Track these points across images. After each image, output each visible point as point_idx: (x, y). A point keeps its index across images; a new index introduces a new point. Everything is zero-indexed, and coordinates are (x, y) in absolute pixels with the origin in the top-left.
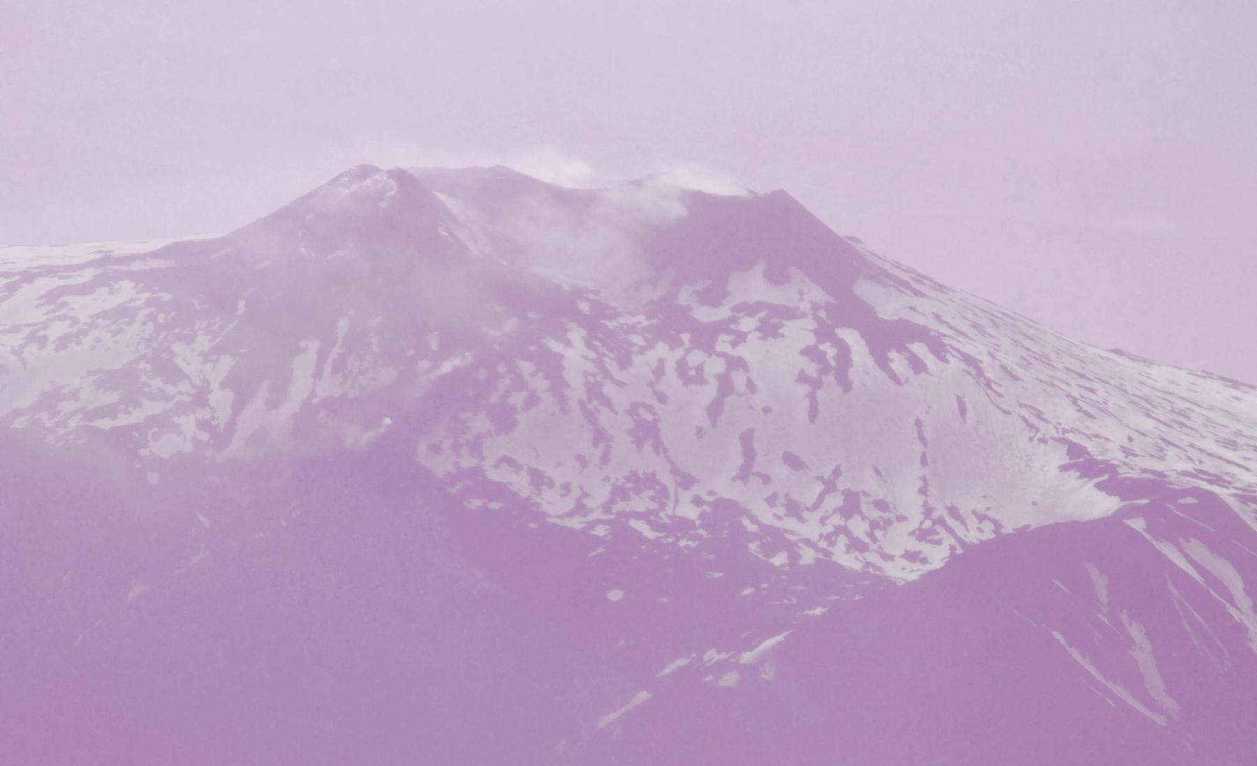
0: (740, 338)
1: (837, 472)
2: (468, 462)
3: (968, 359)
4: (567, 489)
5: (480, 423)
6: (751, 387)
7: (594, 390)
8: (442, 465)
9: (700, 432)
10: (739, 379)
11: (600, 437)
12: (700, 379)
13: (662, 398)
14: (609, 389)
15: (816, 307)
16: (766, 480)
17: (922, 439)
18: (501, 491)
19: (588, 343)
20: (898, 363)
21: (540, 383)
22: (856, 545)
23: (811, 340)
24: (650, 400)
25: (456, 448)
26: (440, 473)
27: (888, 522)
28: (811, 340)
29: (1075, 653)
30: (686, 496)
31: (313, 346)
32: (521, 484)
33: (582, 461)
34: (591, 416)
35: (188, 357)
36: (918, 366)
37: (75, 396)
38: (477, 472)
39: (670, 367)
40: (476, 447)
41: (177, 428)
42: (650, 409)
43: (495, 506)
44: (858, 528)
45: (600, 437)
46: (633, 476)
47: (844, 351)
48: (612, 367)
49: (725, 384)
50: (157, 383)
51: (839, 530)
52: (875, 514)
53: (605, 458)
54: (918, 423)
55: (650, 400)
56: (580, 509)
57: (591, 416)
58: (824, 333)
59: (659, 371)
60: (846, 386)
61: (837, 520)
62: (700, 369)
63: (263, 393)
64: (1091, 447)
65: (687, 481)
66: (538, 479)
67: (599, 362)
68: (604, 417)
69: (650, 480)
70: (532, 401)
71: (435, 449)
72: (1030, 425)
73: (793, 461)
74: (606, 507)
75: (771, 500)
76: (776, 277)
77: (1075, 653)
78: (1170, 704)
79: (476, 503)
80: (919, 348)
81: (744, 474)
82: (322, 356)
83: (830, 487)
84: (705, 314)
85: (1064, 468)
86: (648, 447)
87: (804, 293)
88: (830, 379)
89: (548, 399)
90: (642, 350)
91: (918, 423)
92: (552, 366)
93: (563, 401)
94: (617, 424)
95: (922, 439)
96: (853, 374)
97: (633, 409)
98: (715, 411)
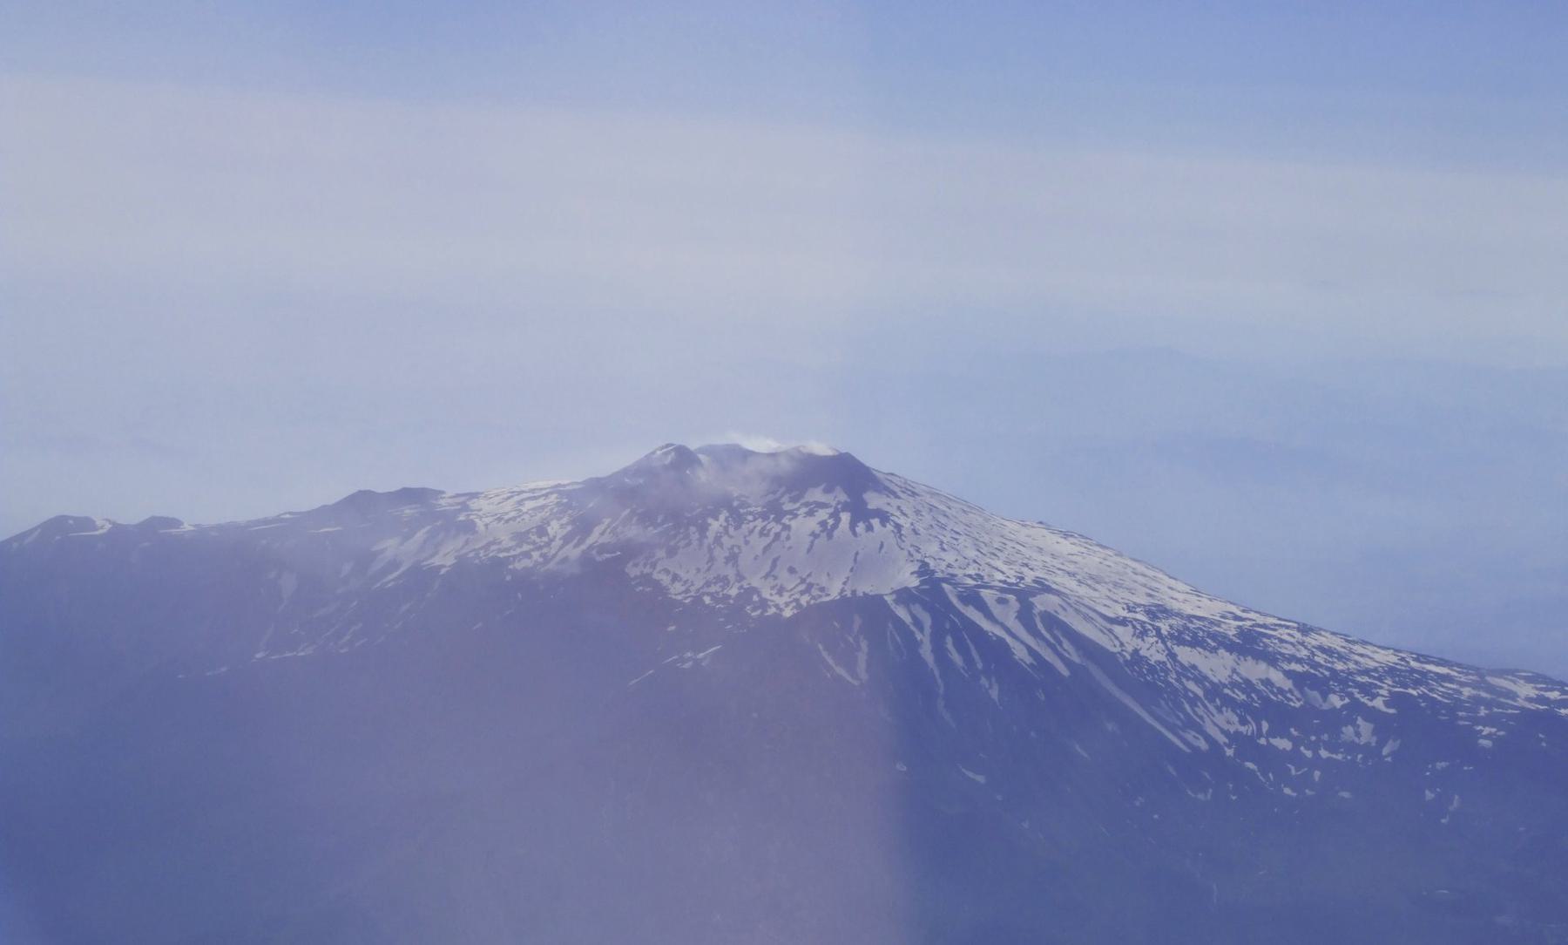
0: (796, 516)
2: (647, 570)
3: (898, 527)
6: (788, 538)
7: (718, 540)
10: (784, 534)
12: (767, 535)
13: (747, 543)
14: (725, 539)
16: (775, 578)
20: (861, 527)
29: (825, 654)
32: (665, 580)
33: (698, 570)
34: (710, 550)
35: (554, 528)
36: (870, 528)
38: (650, 575)
40: (654, 566)
45: (712, 559)
47: (838, 521)
49: (777, 535)
50: (534, 538)
56: (687, 591)
57: (710, 550)
60: (830, 536)
65: (740, 577)
66: (675, 578)
67: (726, 529)
68: (718, 552)
71: (636, 565)
72: (910, 554)
73: (792, 570)
77: (825, 654)
78: (864, 676)
80: (875, 522)
81: (766, 577)
83: (803, 581)
84: (788, 506)
89: (695, 543)
92: (703, 529)
94: (721, 554)
96: (836, 533)
98: (766, 549)
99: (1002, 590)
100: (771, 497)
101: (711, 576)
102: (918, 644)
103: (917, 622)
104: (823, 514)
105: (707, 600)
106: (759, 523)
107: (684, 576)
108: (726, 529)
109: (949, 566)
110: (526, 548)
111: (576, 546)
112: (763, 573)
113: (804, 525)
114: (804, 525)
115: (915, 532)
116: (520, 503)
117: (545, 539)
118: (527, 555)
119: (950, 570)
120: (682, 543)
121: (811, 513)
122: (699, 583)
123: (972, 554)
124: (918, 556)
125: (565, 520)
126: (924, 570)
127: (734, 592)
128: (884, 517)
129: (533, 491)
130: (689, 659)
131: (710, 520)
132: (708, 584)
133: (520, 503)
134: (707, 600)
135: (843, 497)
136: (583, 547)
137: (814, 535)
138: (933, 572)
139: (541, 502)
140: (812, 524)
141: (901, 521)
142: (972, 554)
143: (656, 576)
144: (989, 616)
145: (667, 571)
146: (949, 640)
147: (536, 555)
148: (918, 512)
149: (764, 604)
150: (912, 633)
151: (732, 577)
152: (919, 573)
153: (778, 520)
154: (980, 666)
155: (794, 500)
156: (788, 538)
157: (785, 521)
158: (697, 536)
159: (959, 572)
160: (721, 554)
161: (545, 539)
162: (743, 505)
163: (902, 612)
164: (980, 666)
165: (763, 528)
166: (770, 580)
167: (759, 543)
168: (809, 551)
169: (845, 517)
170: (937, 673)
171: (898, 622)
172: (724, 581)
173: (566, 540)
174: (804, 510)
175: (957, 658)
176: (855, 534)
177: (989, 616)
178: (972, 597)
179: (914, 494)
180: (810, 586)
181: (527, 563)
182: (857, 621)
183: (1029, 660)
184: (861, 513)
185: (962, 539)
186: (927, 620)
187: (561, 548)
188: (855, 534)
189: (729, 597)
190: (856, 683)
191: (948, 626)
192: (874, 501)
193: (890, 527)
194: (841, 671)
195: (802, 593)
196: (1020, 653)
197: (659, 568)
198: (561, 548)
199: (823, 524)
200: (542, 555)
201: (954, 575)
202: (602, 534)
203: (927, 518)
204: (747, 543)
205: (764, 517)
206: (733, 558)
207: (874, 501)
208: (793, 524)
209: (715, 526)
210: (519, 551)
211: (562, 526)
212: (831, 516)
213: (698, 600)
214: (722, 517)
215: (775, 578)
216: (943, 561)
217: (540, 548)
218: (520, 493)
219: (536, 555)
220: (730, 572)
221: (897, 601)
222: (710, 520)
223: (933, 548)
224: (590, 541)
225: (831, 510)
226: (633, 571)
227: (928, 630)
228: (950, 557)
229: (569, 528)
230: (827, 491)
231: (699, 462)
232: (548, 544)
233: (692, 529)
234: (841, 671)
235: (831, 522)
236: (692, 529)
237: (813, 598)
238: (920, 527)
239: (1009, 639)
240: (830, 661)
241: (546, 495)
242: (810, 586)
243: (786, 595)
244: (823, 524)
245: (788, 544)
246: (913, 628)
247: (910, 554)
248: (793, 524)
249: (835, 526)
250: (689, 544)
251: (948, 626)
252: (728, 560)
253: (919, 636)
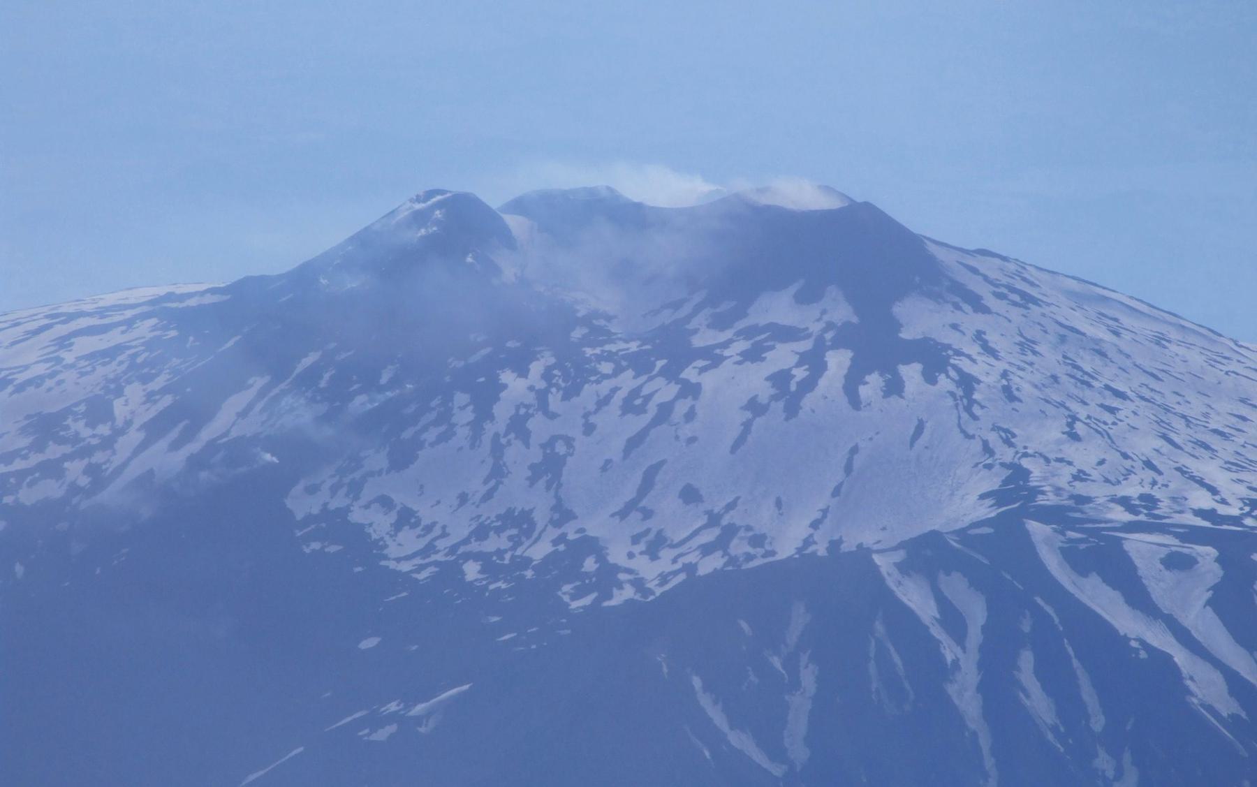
1: (731, 506)
2: (335, 504)
3: (967, 383)
4: (429, 529)
6: (690, 416)
7: (518, 426)
10: (682, 408)
12: (641, 410)
13: (589, 429)
17: (848, 469)
19: (547, 375)
20: (872, 386)
21: (464, 417)
29: (705, 701)
30: (553, 533)
31: (258, 382)
32: (380, 523)
33: (463, 499)
36: (894, 387)
40: (355, 489)
42: (569, 441)
45: (498, 472)
53: (488, 496)
54: (855, 450)
56: (429, 549)
57: (498, 449)
60: (792, 410)
63: (174, 434)
65: (562, 514)
66: (406, 518)
67: (542, 396)
71: (312, 490)
72: (987, 449)
73: (690, 495)
77: (705, 701)
78: (799, 753)
79: (316, 546)
80: (911, 373)
82: (262, 394)
83: (713, 519)
86: (541, 484)
89: (463, 433)
91: (855, 450)
94: (520, 458)
96: (808, 401)
97: (553, 439)
98: (635, 442)
99: (1192, 535)
100: (666, 317)
101: (491, 512)
102: (946, 672)
103: (953, 620)
104: (783, 356)
105: (472, 571)
106: (627, 381)
107: (426, 514)
108: (542, 396)
109: (1080, 476)
111: (176, 446)
112: (617, 505)
113: (731, 385)
114: (731, 385)
115: (1009, 394)
116: (63, 342)
117: (104, 430)
118: (52, 469)
119: (1081, 488)
120: (430, 435)
121: (754, 355)
122: (461, 529)
123: (1146, 444)
124: (1007, 455)
126: (1015, 490)
127: (539, 551)
128: (934, 358)
129: (102, 312)
130: (393, 718)
131: (507, 377)
132: (481, 533)
133: (63, 342)
134: (472, 571)
135: (842, 312)
136: (193, 447)
137: (755, 407)
138: (1037, 491)
139: (115, 338)
140: (755, 380)
141: (983, 370)
142: (1146, 444)
143: (357, 516)
144: (1139, 599)
145: (386, 503)
146: (1027, 660)
148: (1027, 345)
149: (608, 577)
150: (938, 643)
151: (541, 517)
152: (998, 497)
153: (671, 374)
154: (1098, 723)
155: (719, 323)
156: (690, 416)
157: (690, 374)
158: (468, 415)
159: (1099, 492)
160: (520, 458)
161: (104, 430)
162: (599, 335)
163: (916, 597)
164: (1098, 723)
165: (635, 393)
166: (635, 524)
167: (616, 428)
168: (735, 448)
169: (838, 362)
170: (985, 742)
171: (902, 617)
172: (521, 523)
173: (155, 429)
174: (742, 345)
175: (1039, 703)
176: (855, 402)
177: (1139, 599)
178: (1103, 556)
179: (1028, 299)
180: (730, 532)
181: (51, 489)
182: (800, 618)
183: (1227, 706)
184: (879, 349)
185: (1125, 409)
186: (976, 612)
187: (143, 446)
188: (855, 402)
189: (526, 562)
190: (778, 770)
192: (919, 319)
193: (945, 383)
194: (741, 741)
195: (706, 550)
196: (1205, 687)
197: (368, 493)
198: (143, 446)
199: (780, 379)
200: (92, 470)
201: (1083, 500)
202: (243, 414)
203: (1050, 357)
204: (589, 429)
205: (640, 364)
206: (550, 468)
207: (919, 319)
208: (709, 381)
209: (515, 387)
210: (35, 459)
211: (150, 398)
212: (803, 359)
213: (450, 572)
214: (536, 368)
215: (648, 514)
216: (1066, 462)
217: (87, 451)
218: (71, 317)
220: (540, 504)
221: (904, 568)
222: (507, 377)
223: (1050, 434)
224: (206, 435)
225: (805, 346)
226: (301, 504)
227: (975, 636)
228: (1085, 455)
229: (168, 400)
230: (803, 298)
231: (508, 240)
232: (108, 443)
233: (461, 398)
234: (741, 741)
235: (800, 374)
236: (461, 398)
237: (733, 560)
238: (1024, 384)
239: (1180, 656)
240: (718, 718)
241: (129, 323)
242: (730, 532)
243: (666, 554)
244: (780, 379)
245: (687, 431)
246: (937, 632)
247: (987, 449)
248: (709, 381)
249: (809, 385)
250: (444, 438)
251: (1026, 627)
252: (536, 473)
253: (950, 652)
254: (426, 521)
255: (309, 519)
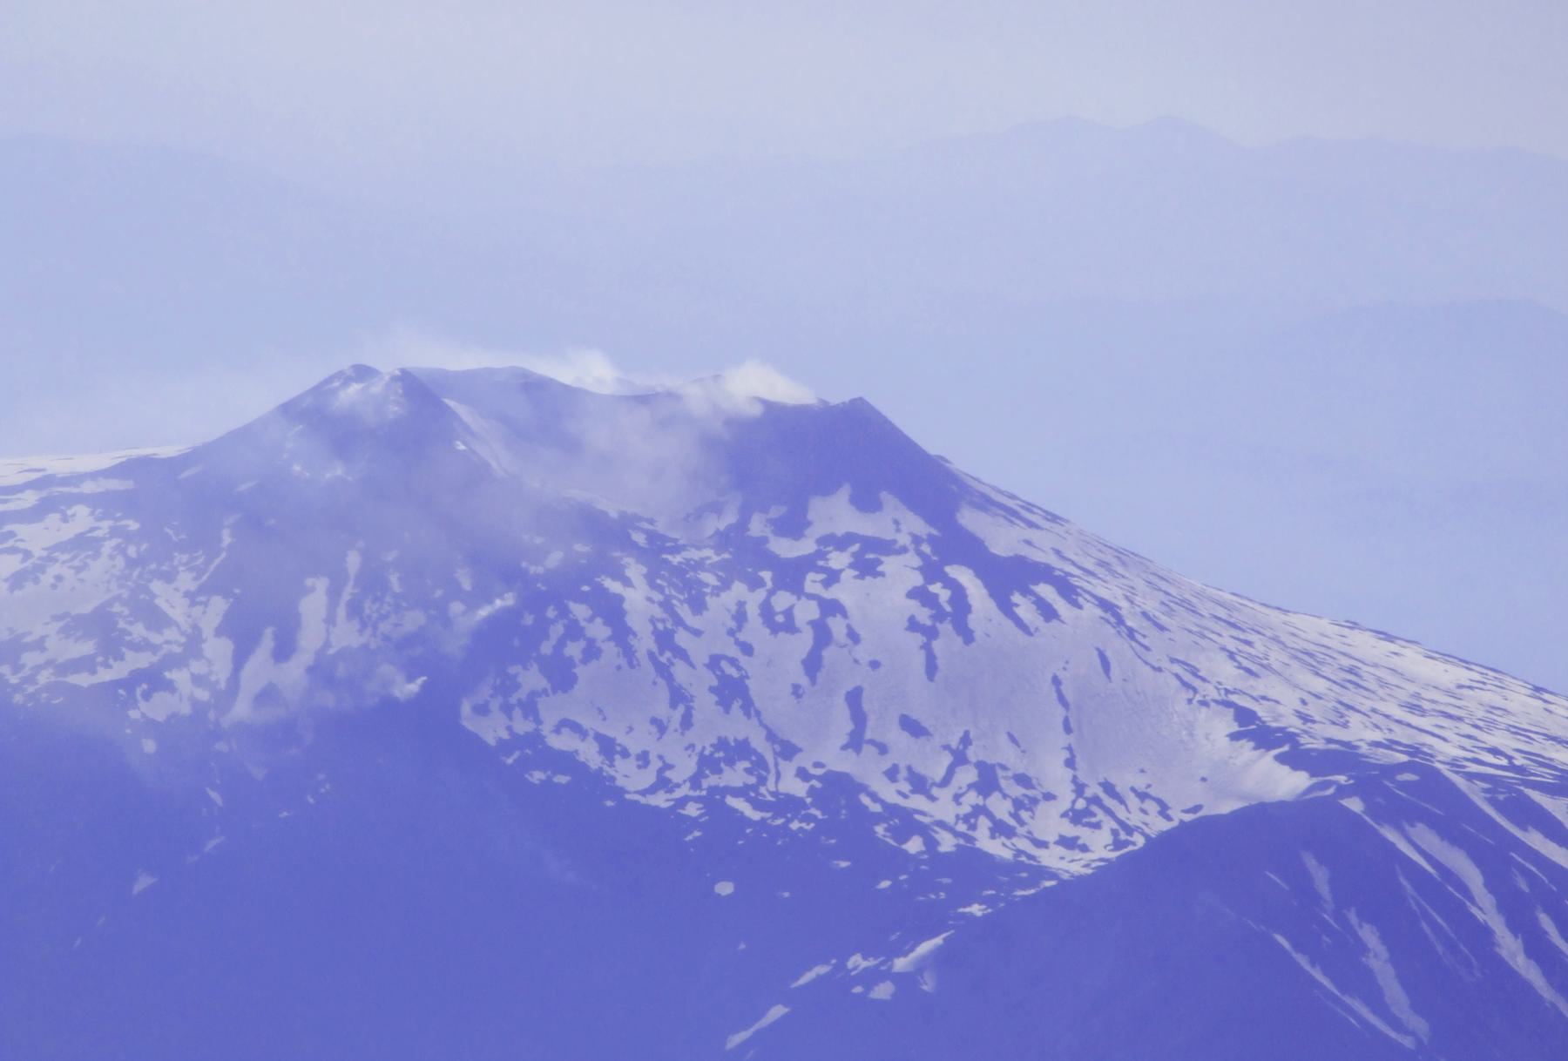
0: (832, 577)
1: (966, 740)
2: (523, 726)
3: (1105, 605)
5: (531, 679)
6: (854, 636)
7: (664, 639)
8: (492, 730)
9: (796, 691)
10: (837, 626)
11: (678, 696)
12: (790, 627)
13: (747, 649)
14: (682, 638)
15: (917, 540)
16: (883, 749)
17: (1062, 699)
18: (566, 761)
19: (651, 580)
21: (599, 630)
22: (1000, 829)
23: (918, 580)
24: (733, 651)
25: (507, 709)
26: (491, 741)
27: (1034, 801)
28: (918, 580)
29: (1302, 961)
30: (789, 769)
31: (321, 585)
32: (589, 754)
33: (661, 726)
34: (664, 671)
35: (170, 599)
36: (1049, 613)
37: (40, 645)
38: (535, 739)
39: (753, 610)
40: (530, 708)
41: (170, 687)
42: (733, 662)
43: (562, 779)
44: (1001, 808)
45: (678, 696)
46: (722, 744)
47: (959, 594)
48: (684, 612)
49: (822, 635)
50: (138, 630)
51: (979, 811)
52: (1018, 791)
53: (687, 722)
54: (1056, 681)
55: (733, 651)
56: (663, 784)
57: (664, 671)
58: (932, 571)
59: (740, 617)
60: (968, 636)
61: (972, 798)
62: (789, 613)
64: (1261, 711)
66: (608, 747)
67: (666, 605)
68: (680, 671)
69: (742, 750)
70: (592, 652)
71: (482, 710)
73: (913, 727)
74: (695, 781)
75: (892, 774)
76: (866, 502)
77: (1302, 961)
78: (1420, 1025)
79: (537, 776)
80: (1046, 591)
81: (855, 742)
82: (334, 593)
83: (960, 759)
84: (785, 548)
85: (1234, 737)
86: (736, 706)
87: (898, 522)
88: (946, 628)
89: (610, 650)
90: (717, 591)
91: (1056, 681)
92: (612, 611)
93: (629, 653)
94: (698, 682)
95: (1062, 699)
96: (973, 621)
97: (714, 662)
98: (812, 664)
110: (143, 660)
125: (186, 581)
147: (180, 677)
157: (812, 583)
191: (1523, 885)
206: (732, 691)
219: (180, 677)
254: (635, 749)
255: (504, 747)
